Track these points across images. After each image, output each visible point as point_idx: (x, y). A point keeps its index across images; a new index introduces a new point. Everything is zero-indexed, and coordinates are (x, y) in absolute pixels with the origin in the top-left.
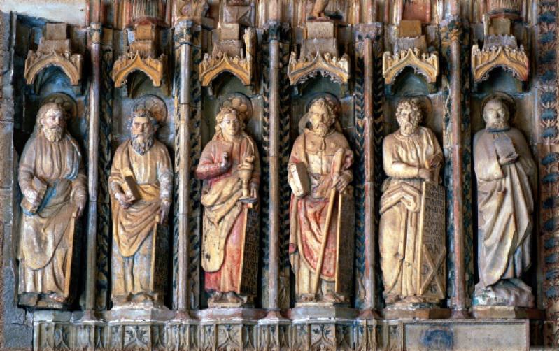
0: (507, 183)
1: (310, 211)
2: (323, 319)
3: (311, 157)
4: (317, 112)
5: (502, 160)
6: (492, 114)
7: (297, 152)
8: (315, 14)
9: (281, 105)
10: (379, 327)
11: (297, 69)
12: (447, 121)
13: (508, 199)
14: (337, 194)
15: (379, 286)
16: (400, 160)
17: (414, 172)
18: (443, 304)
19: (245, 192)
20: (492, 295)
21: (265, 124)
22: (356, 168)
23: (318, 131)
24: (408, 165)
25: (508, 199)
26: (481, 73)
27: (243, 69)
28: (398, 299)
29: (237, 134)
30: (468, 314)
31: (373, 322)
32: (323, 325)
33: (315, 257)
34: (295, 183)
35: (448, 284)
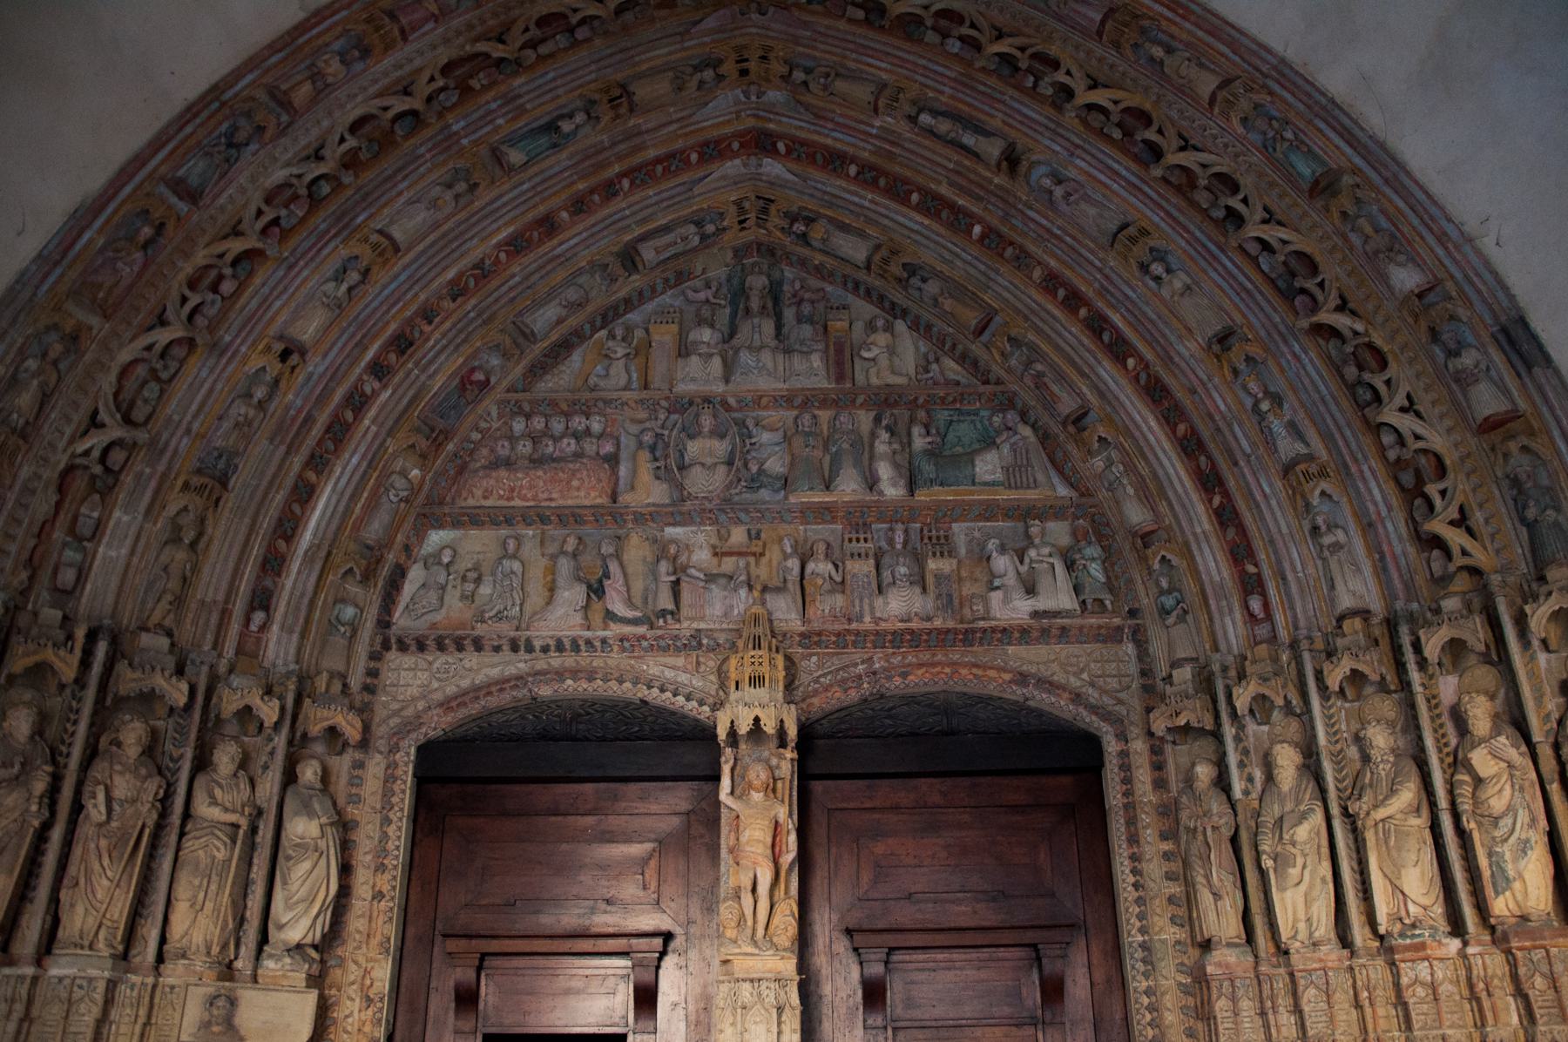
0: (322, 844)
1: (103, 843)
2: (93, 972)
3: (118, 780)
4: (132, 734)
5: (324, 820)
6: (309, 773)
7: (99, 770)
8: (150, 624)
9: (95, 713)
10: (155, 987)
11: (128, 680)
12: (266, 767)
13: (323, 861)
14: (143, 826)
15: (163, 940)
16: (214, 802)
17: (232, 818)
18: (230, 966)
19: (34, 808)
20: (288, 960)
21: (66, 730)
22: (165, 801)
23: (132, 751)
24: (226, 810)
25: (323, 861)
26: (318, 728)
27: (67, 667)
28: (184, 956)
29: (32, 738)
30: (255, 979)
31: (150, 980)
32: (91, 980)
33: (99, 896)
34: (96, 809)
35: (237, 946)
